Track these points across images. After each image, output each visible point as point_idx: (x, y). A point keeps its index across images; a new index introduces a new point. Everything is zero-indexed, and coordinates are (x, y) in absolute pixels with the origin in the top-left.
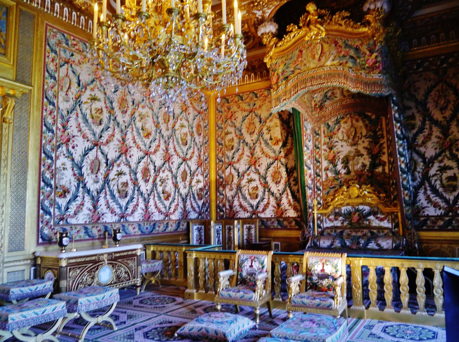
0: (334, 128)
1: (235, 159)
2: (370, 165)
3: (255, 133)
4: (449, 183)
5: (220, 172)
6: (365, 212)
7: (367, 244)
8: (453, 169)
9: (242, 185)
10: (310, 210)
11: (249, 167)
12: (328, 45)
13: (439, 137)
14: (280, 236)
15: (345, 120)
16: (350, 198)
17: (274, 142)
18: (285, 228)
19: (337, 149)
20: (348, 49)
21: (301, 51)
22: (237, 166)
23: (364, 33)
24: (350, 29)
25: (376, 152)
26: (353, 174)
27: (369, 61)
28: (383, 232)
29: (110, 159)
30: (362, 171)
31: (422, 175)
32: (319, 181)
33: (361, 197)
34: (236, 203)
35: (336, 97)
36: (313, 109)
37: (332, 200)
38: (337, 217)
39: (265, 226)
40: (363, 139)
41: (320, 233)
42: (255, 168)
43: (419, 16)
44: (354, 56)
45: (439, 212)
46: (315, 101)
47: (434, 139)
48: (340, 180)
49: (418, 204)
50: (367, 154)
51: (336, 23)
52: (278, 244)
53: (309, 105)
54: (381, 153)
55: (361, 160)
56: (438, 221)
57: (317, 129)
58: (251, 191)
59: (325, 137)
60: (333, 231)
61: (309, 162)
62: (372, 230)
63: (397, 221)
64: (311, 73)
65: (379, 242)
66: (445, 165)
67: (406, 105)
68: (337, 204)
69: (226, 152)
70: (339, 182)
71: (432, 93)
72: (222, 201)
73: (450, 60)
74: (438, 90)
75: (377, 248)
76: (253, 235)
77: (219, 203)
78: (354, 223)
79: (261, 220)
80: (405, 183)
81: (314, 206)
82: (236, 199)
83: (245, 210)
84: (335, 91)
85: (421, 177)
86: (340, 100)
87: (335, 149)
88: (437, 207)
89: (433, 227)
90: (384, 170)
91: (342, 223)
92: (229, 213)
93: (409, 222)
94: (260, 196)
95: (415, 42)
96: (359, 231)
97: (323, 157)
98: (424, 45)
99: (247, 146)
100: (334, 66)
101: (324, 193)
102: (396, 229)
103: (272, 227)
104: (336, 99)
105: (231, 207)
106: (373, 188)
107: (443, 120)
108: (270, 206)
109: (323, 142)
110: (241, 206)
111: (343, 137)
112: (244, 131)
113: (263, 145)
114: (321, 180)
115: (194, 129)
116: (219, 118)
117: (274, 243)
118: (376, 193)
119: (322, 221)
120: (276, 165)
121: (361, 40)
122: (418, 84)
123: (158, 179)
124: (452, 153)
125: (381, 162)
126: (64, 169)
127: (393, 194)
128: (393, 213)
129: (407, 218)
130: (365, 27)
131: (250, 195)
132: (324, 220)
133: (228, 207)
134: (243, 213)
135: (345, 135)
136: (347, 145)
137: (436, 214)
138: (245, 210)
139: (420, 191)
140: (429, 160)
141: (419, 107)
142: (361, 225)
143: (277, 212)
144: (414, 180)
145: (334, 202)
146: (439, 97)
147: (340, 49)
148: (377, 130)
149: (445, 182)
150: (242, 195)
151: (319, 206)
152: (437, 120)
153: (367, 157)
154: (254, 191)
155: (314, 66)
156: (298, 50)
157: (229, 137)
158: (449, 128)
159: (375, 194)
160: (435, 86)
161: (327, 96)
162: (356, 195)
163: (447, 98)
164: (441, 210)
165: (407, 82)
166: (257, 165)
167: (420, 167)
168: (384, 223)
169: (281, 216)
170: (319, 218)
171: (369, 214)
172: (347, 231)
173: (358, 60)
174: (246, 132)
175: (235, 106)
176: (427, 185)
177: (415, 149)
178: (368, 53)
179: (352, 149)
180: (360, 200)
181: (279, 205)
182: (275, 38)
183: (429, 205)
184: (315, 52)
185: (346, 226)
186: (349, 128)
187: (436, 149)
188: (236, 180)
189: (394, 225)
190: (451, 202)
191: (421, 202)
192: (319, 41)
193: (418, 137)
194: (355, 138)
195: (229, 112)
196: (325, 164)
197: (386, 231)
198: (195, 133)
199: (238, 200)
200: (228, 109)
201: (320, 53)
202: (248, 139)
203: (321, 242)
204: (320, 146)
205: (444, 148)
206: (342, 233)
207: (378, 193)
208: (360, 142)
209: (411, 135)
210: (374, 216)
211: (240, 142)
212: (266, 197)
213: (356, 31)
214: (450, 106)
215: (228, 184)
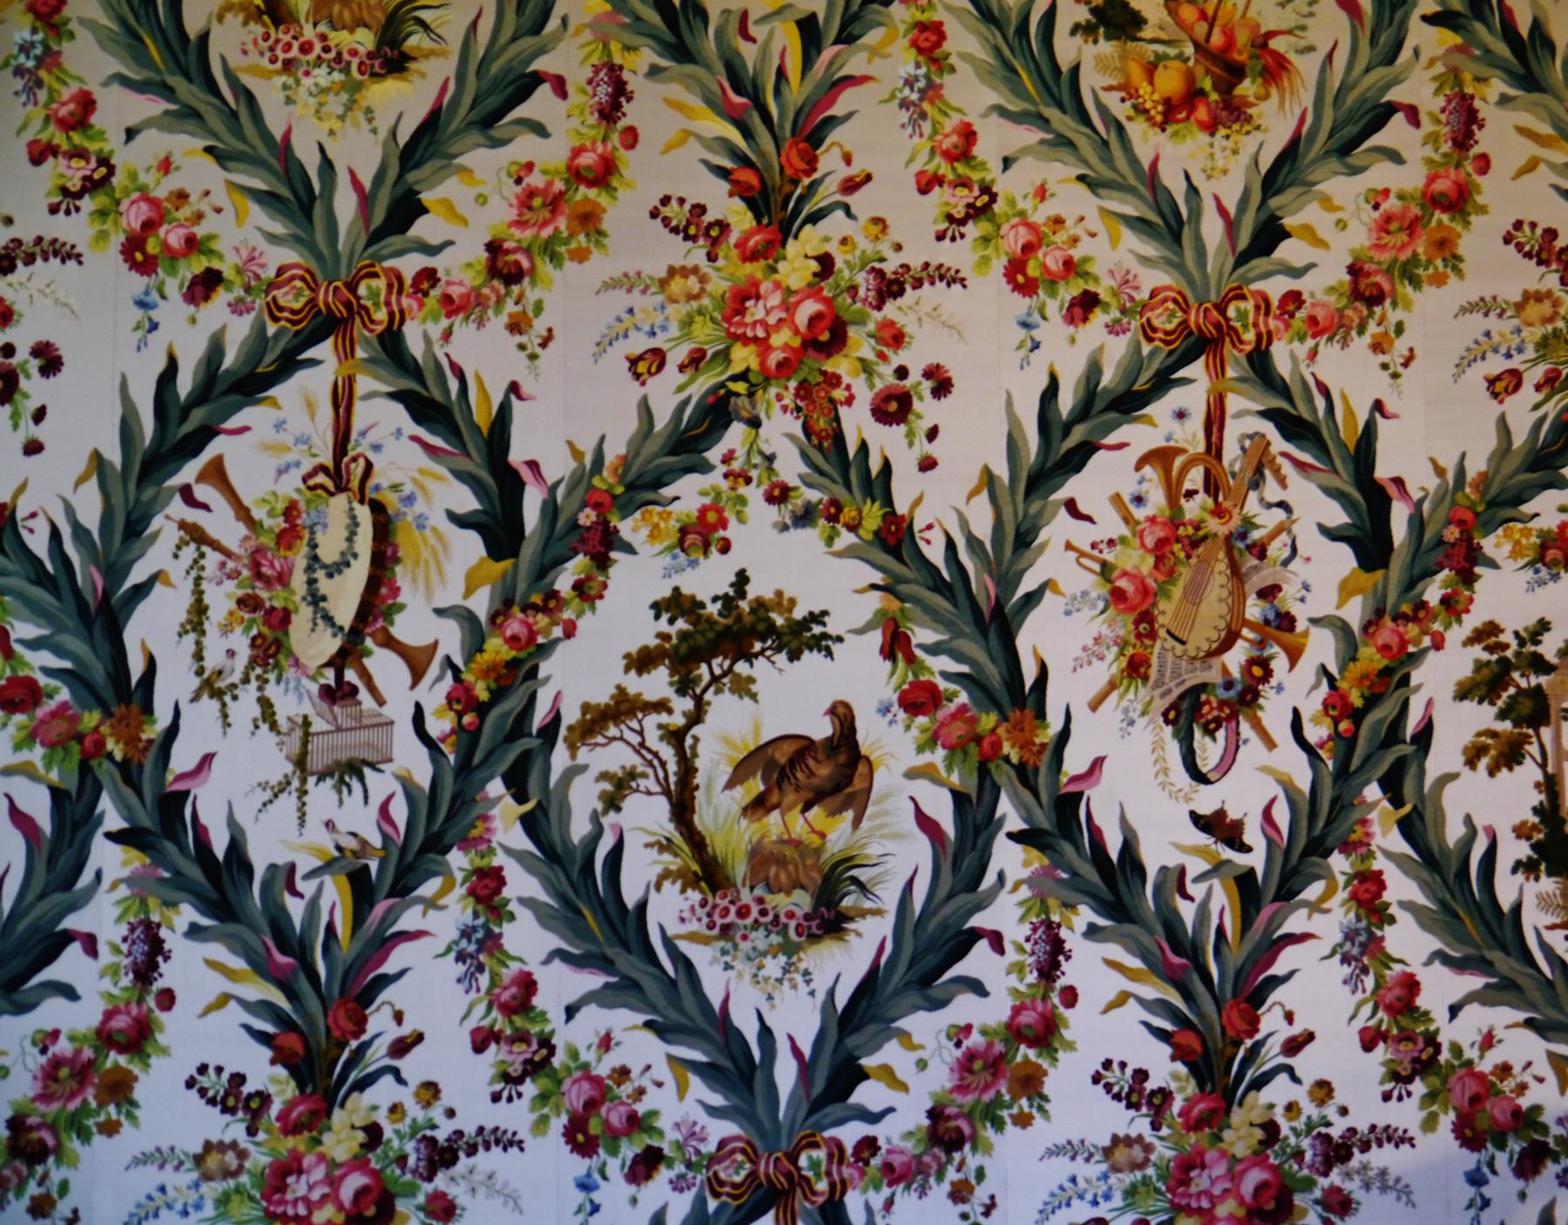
8: (823, 644)
31: (461, 699)
66: (742, 579)
85: (438, 726)
88: (614, 1137)
124: (839, 438)
140: (551, 510)
183: (516, 1116)
191: (414, 1066)
205: (744, 357)
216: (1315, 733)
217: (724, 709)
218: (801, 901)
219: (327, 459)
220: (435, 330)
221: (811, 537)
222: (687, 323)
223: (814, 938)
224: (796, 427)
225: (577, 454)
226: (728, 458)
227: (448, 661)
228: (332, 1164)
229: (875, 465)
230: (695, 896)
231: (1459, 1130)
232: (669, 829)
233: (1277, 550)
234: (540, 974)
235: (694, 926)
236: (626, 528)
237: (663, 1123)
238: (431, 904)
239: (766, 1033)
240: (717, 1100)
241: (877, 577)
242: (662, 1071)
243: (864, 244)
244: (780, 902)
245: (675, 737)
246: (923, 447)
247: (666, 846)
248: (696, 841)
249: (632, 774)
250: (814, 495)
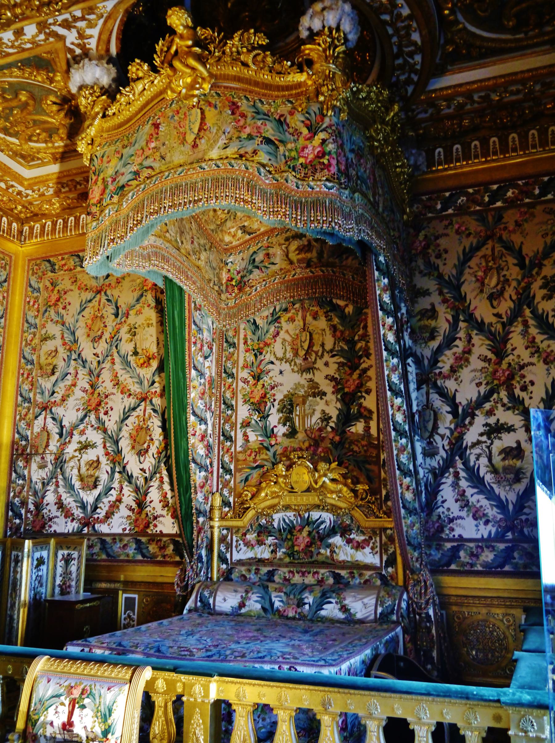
0: (267, 332)
1: (58, 397)
2: (338, 416)
3: (104, 338)
4: (507, 462)
5: (23, 424)
6: (323, 526)
7: (320, 607)
8: (514, 430)
9: (67, 456)
10: (201, 520)
11: (85, 416)
12: (216, 112)
13: (485, 359)
14: (139, 579)
15: (289, 315)
16: (292, 490)
17: (142, 361)
18: (151, 560)
19: (271, 378)
20: (259, 123)
21: (156, 126)
22: (59, 411)
23: (299, 85)
24: (266, 77)
25: (352, 387)
26: (301, 436)
27: (306, 151)
28: (361, 575)
30: (320, 430)
31: (450, 443)
32: (228, 451)
33: (315, 490)
34: (50, 498)
35: (273, 264)
36: (224, 288)
37: (253, 496)
38: (263, 537)
39: (108, 555)
40: (326, 357)
41: (223, 575)
43: (442, 89)
44: (273, 138)
45: (485, 531)
46: (229, 270)
47: (475, 363)
48: (272, 450)
49: (441, 510)
50: (333, 393)
51: (236, 59)
52: (134, 598)
53: (210, 275)
54: (363, 390)
55: (320, 405)
56: (483, 551)
57: (231, 333)
58: (83, 470)
59: (246, 351)
60: (253, 572)
61: (200, 404)
62: (337, 571)
63: (391, 550)
64: (175, 178)
65: (348, 602)
66: (498, 420)
67: (418, 286)
68: (263, 505)
69: (39, 378)
70: (270, 454)
71: (473, 263)
72: (20, 492)
73: (509, 194)
74: (484, 256)
75: (341, 616)
76: (74, 575)
77: (14, 497)
78: (298, 552)
79: (102, 539)
80: (404, 458)
81: (212, 509)
82: (51, 488)
83: (68, 514)
84: (271, 251)
85: (447, 448)
86: (281, 269)
87: (266, 379)
89: (472, 565)
90: (367, 428)
91: (274, 552)
92: (34, 521)
93: (416, 554)
94: (102, 483)
95: (439, 152)
96: (309, 573)
97: (240, 396)
98: (458, 160)
99: (84, 367)
100: (225, 161)
101: (238, 480)
102: (390, 570)
103: (122, 558)
104: (274, 268)
105: (38, 506)
106: (344, 471)
107: (494, 320)
108: (122, 507)
109: (241, 363)
110: (60, 505)
111: (285, 353)
112: (81, 333)
113: (118, 367)
114: (233, 449)
116: (31, 303)
117: (125, 595)
118: (349, 481)
119: (229, 547)
120: (141, 413)
121: (291, 102)
122: (443, 242)
125: (362, 410)
127: (385, 486)
128: (385, 529)
129: (409, 544)
130: (302, 71)
131: (82, 479)
132: (234, 544)
133: (31, 507)
134: (64, 520)
135: (289, 348)
136: (292, 369)
137: (479, 536)
138: (68, 514)
139: (444, 480)
140: (463, 410)
141: (445, 291)
142: (315, 558)
143: (136, 520)
144: (430, 453)
145: (256, 500)
146: (487, 270)
147: (242, 123)
148: (356, 338)
149: (497, 459)
150: (65, 479)
151: (227, 509)
152: (482, 320)
153: (334, 397)
155: (181, 162)
156: (150, 122)
157: (49, 346)
158: (505, 340)
159: (346, 485)
160: (478, 248)
161: (254, 260)
162: (305, 487)
163: (505, 272)
164: (490, 526)
165: (421, 237)
166: (102, 411)
168: (364, 554)
169: (143, 533)
170: (223, 539)
171: (332, 532)
172: (283, 572)
173: (282, 149)
174: (85, 336)
175: (67, 278)
176: (459, 465)
177: (435, 385)
178: (305, 131)
179: (302, 379)
180: (313, 499)
181: (141, 504)
182: (104, 97)
183: (464, 514)
184: (187, 127)
185: (280, 559)
186: (297, 332)
187: (479, 385)
188: (53, 446)
189: (385, 558)
190: (511, 507)
191: (446, 505)
192: (195, 100)
193: (443, 358)
194: (310, 355)
195: (53, 290)
197: (368, 574)
199: (56, 491)
200: (52, 284)
201: (196, 130)
202: (88, 353)
203: (219, 597)
204: (234, 371)
205: (496, 382)
206: (271, 574)
207: (353, 483)
208: (320, 364)
209: (427, 353)
210: (341, 536)
211: (69, 357)
212: (116, 485)
213: (279, 80)
214: (510, 291)
215: (37, 453)
216: (155, 456)
217: (497, 442)
218: (512, 476)
219: (425, 403)
220: (442, 381)
221: (510, 412)
222: (486, 377)
223: (515, 483)
224: (506, 393)
225: (467, 400)
226: (494, 400)
227: (448, 437)
228: (433, 522)
229: (521, 399)
230: (493, 475)
231: (171, 516)
232: (488, 463)
233: (152, 429)
234: (466, 490)
235: (493, 481)
236: (477, 412)
237: (490, 515)
238: (447, 478)
239: (507, 500)
240: (499, 511)
241: (523, 418)
242: (488, 506)
243: (516, 360)
244: (509, 476)
245: (488, 447)
246: (530, 395)
247: (487, 466)
248: (492, 465)
249: (481, 454)
250: (510, 405)
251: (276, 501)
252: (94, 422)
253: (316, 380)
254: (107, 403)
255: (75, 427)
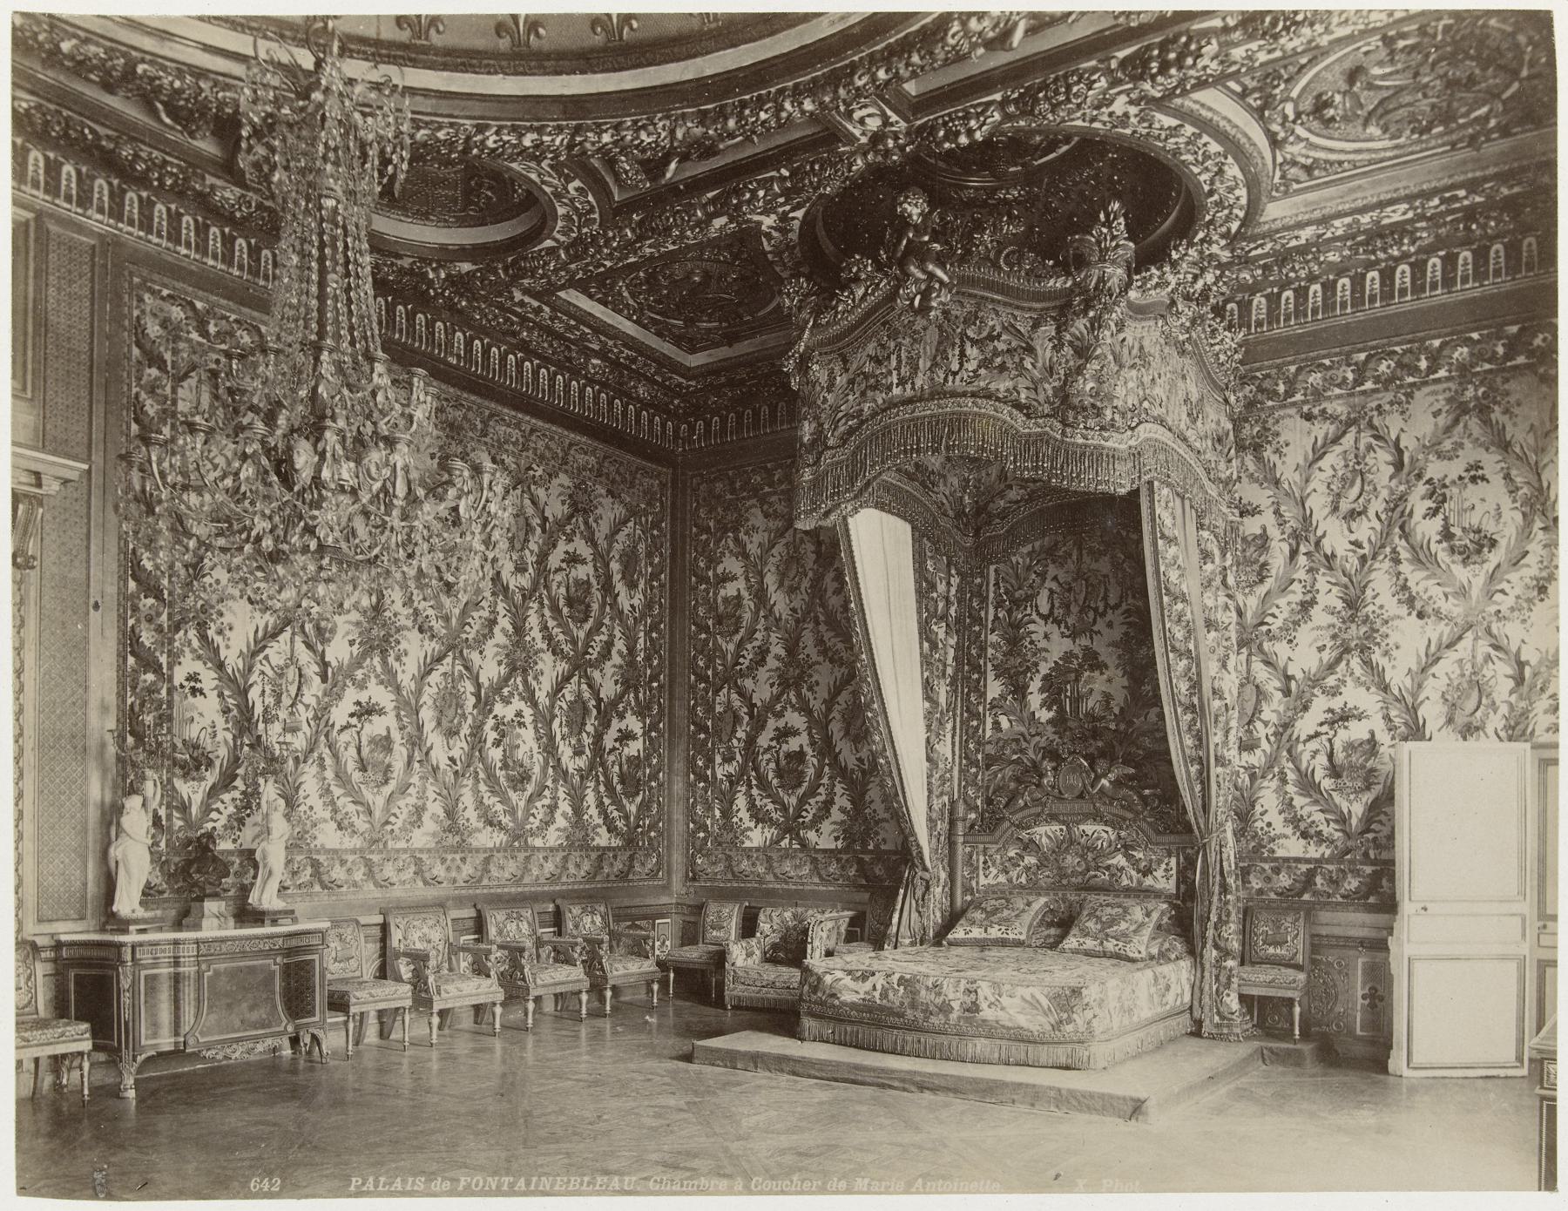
11: (782, 694)
22: (748, 683)
29: (334, 664)
33: (1092, 797)
34: (741, 802)
42: (799, 695)
105: (727, 813)
111: (1053, 606)
115: (615, 566)
123: (491, 722)
126: (194, 691)
154: (793, 765)
157: (730, 590)
167: (1273, 710)
196: (994, 688)
198: (617, 577)
217: (1341, 732)
245: (1330, 740)
251: (1039, 809)
252: (794, 700)
253: (1096, 647)
254: (811, 676)
255: (769, 707)
